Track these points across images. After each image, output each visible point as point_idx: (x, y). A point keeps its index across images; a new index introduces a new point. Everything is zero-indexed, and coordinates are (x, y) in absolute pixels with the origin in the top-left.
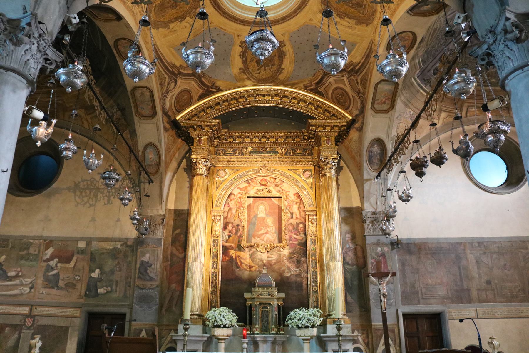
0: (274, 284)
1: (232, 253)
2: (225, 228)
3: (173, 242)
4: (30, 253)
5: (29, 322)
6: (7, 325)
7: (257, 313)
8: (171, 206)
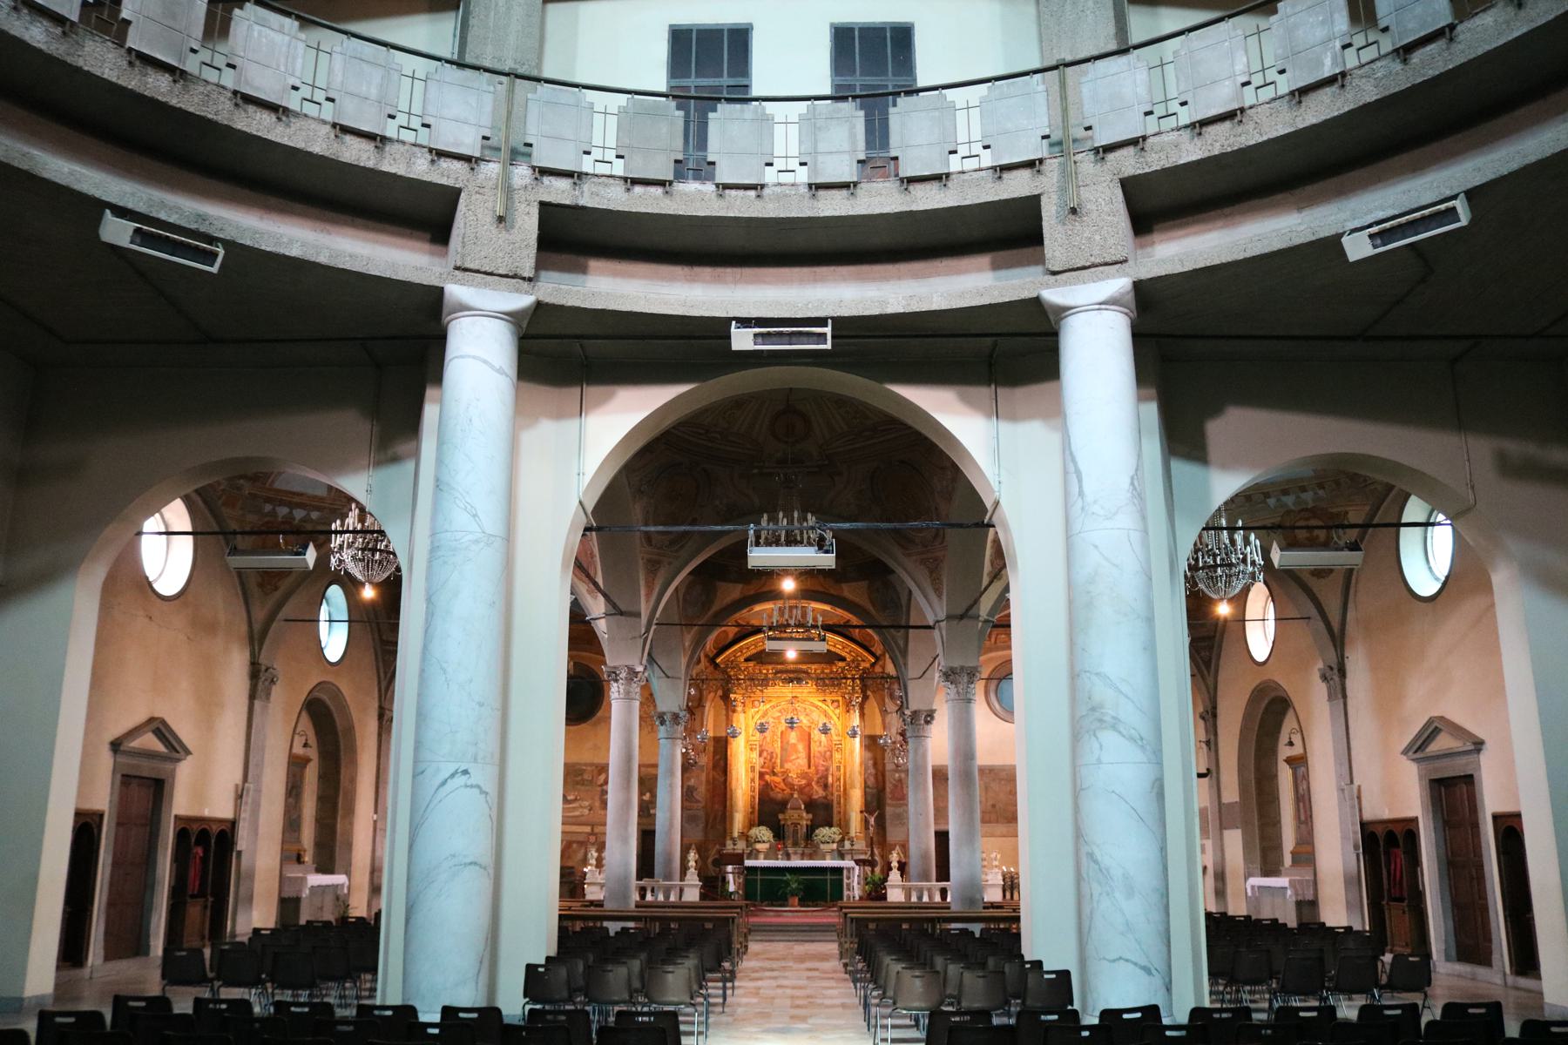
0: (803, 807)
1: (767, 777)
2: (760, 755)
3: (715, 767)
5: (592, 839)
6: (574, 842)
7: (789, 831)
8: (711, 734)
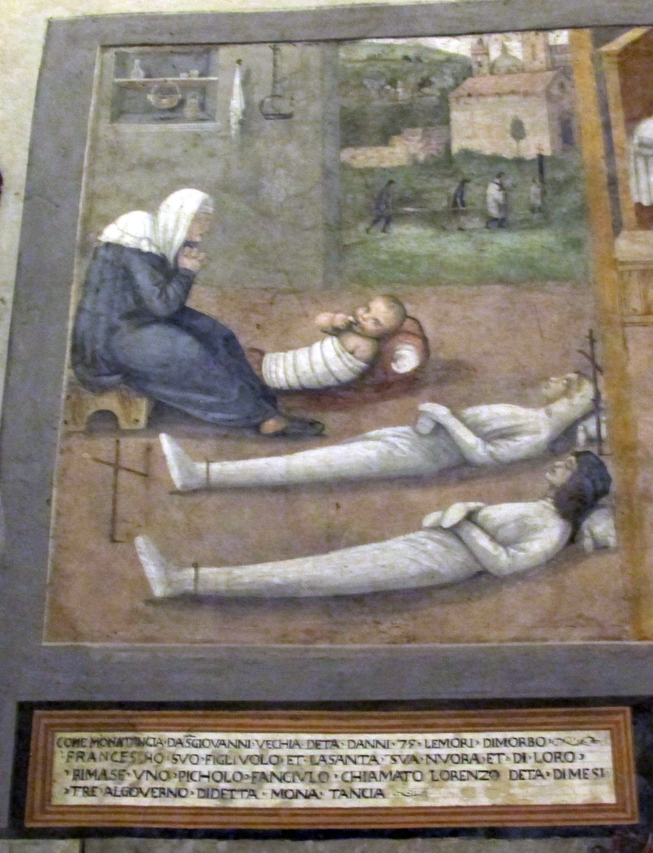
4: (468, 155)
